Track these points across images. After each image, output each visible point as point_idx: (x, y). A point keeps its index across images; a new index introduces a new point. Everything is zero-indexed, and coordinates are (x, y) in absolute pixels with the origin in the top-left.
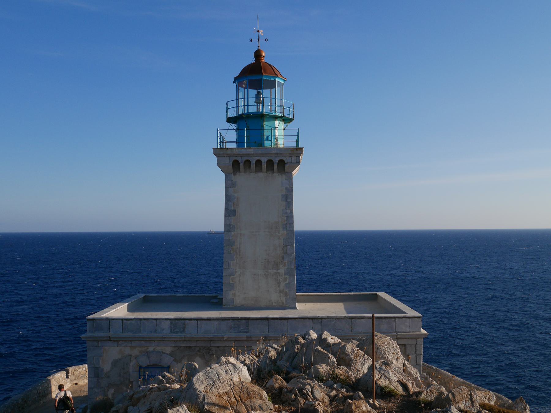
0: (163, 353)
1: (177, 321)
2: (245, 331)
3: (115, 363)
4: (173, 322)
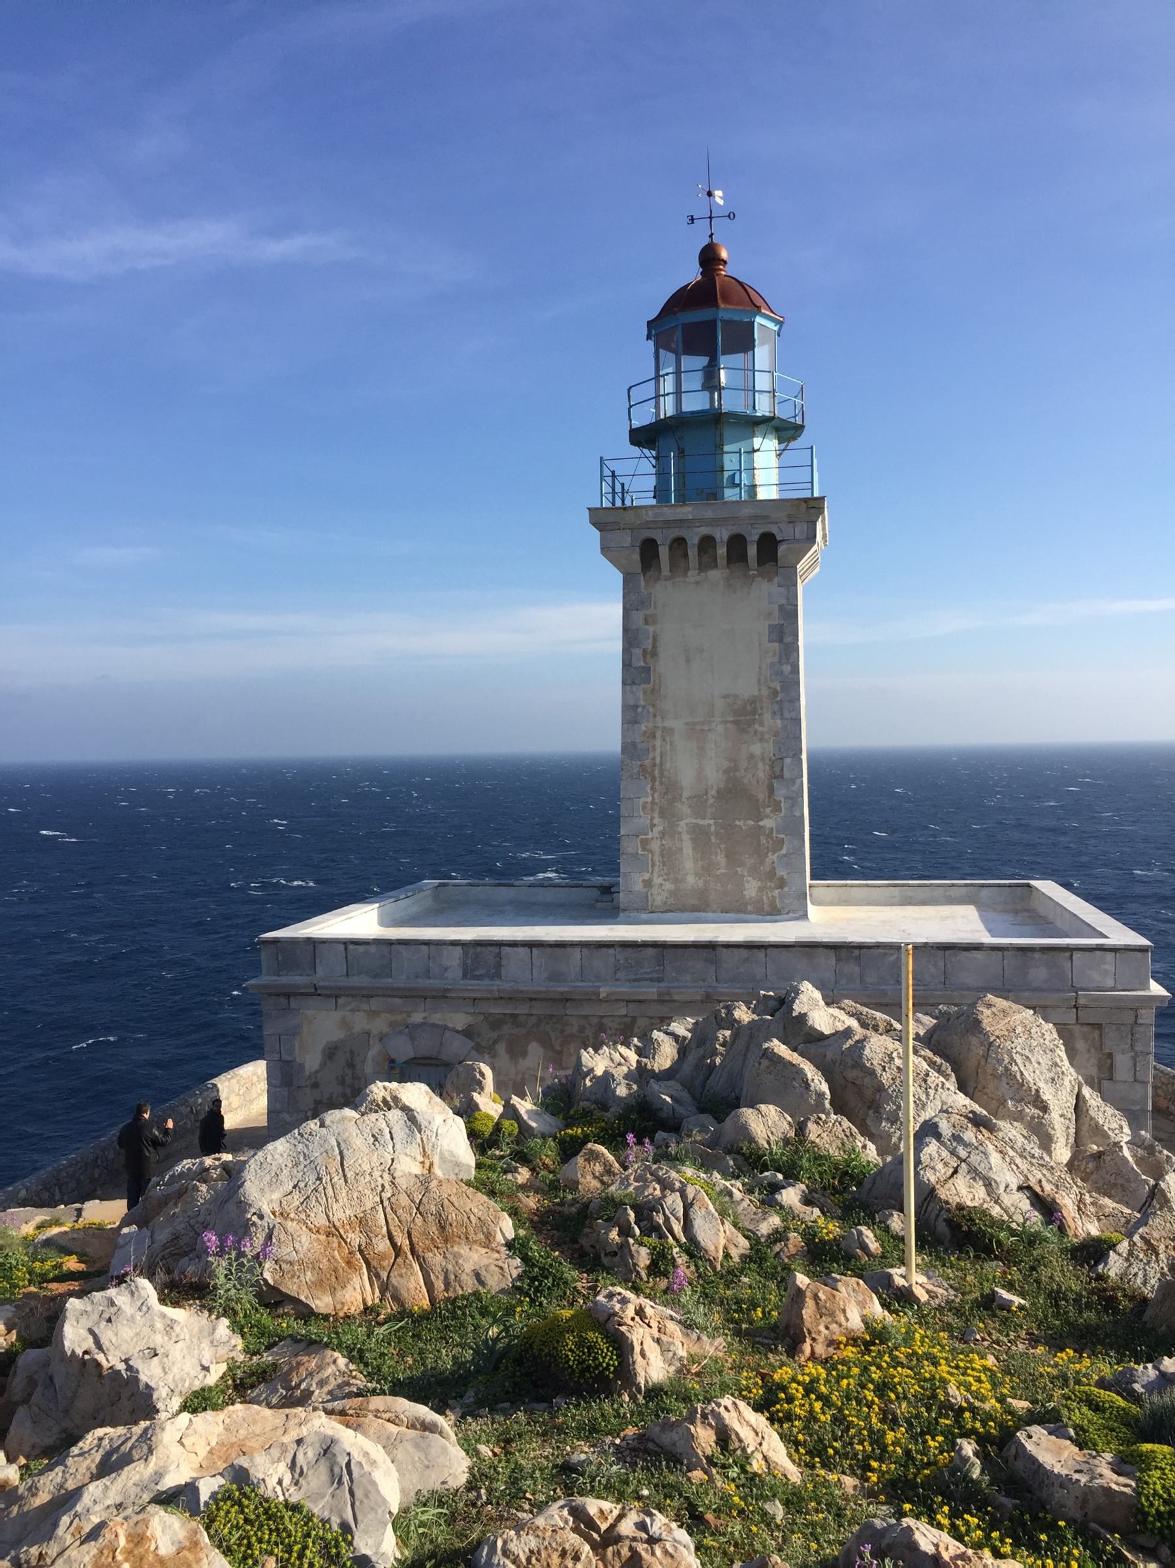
0: (446, 1028)
1: (479, 949)
2: (655, 975)
3: (331, 1052)
4: (471, 951)
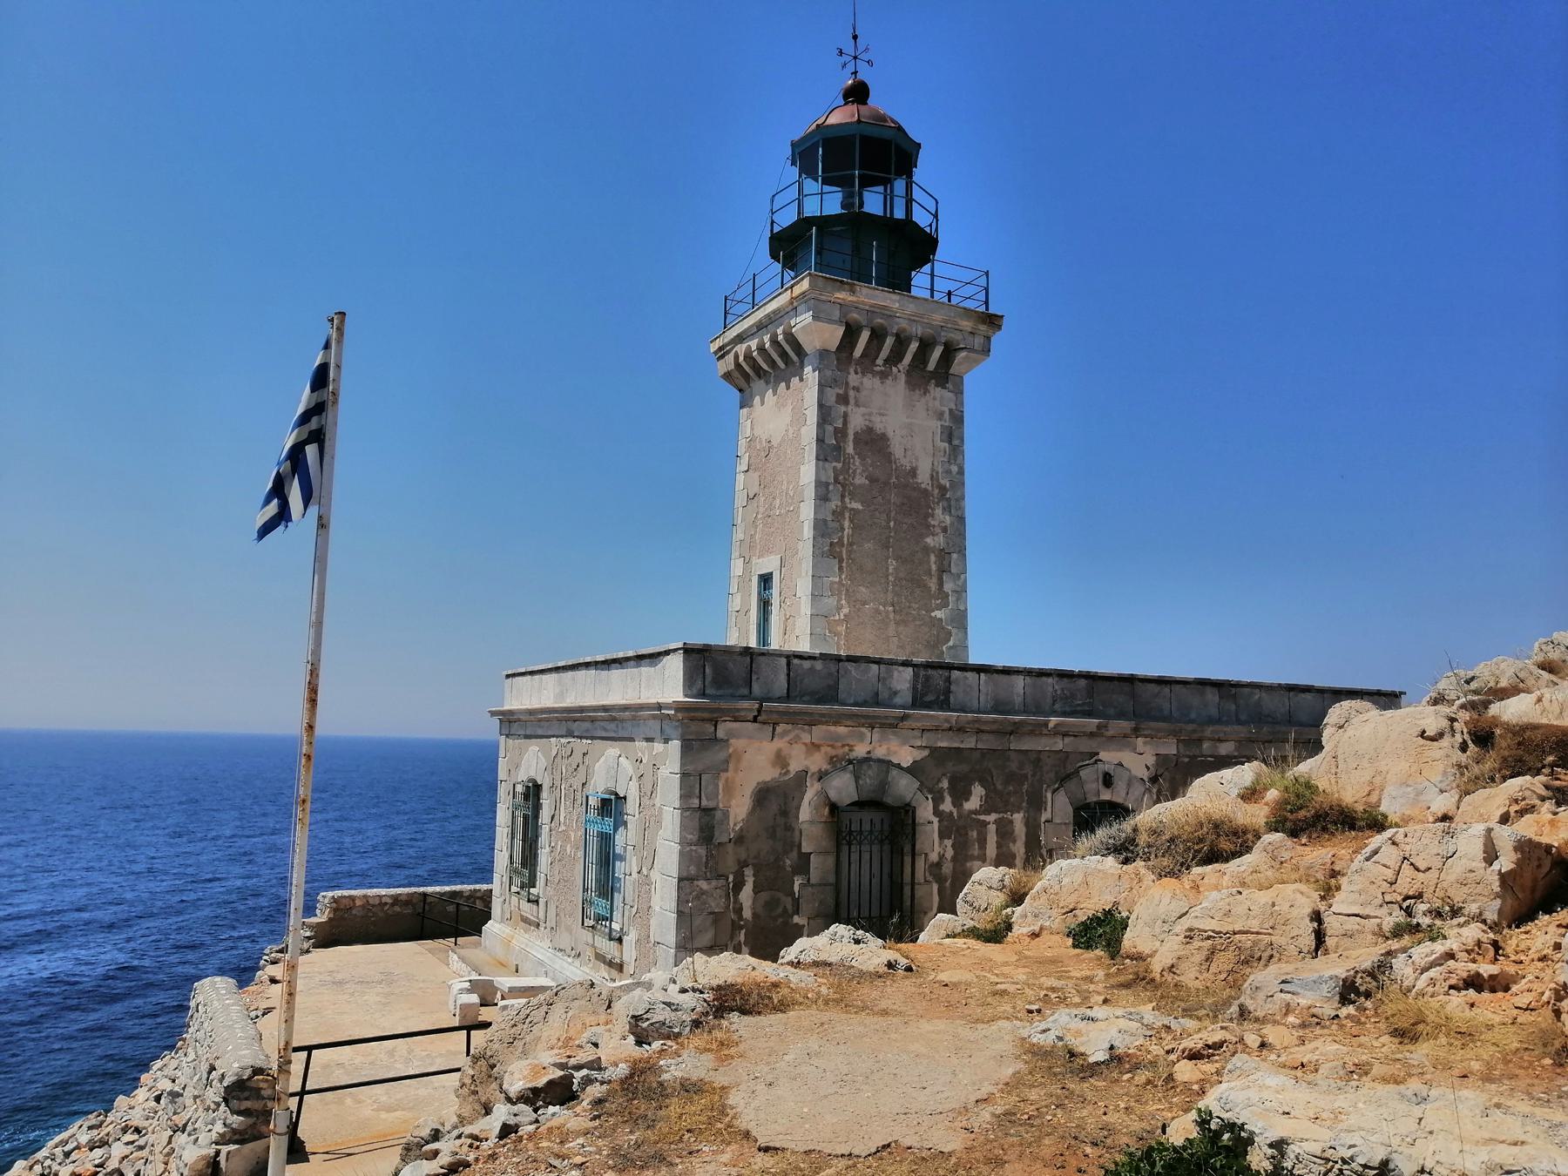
1: (930, 672)
3: (763, 795)
4: (922, 673)
